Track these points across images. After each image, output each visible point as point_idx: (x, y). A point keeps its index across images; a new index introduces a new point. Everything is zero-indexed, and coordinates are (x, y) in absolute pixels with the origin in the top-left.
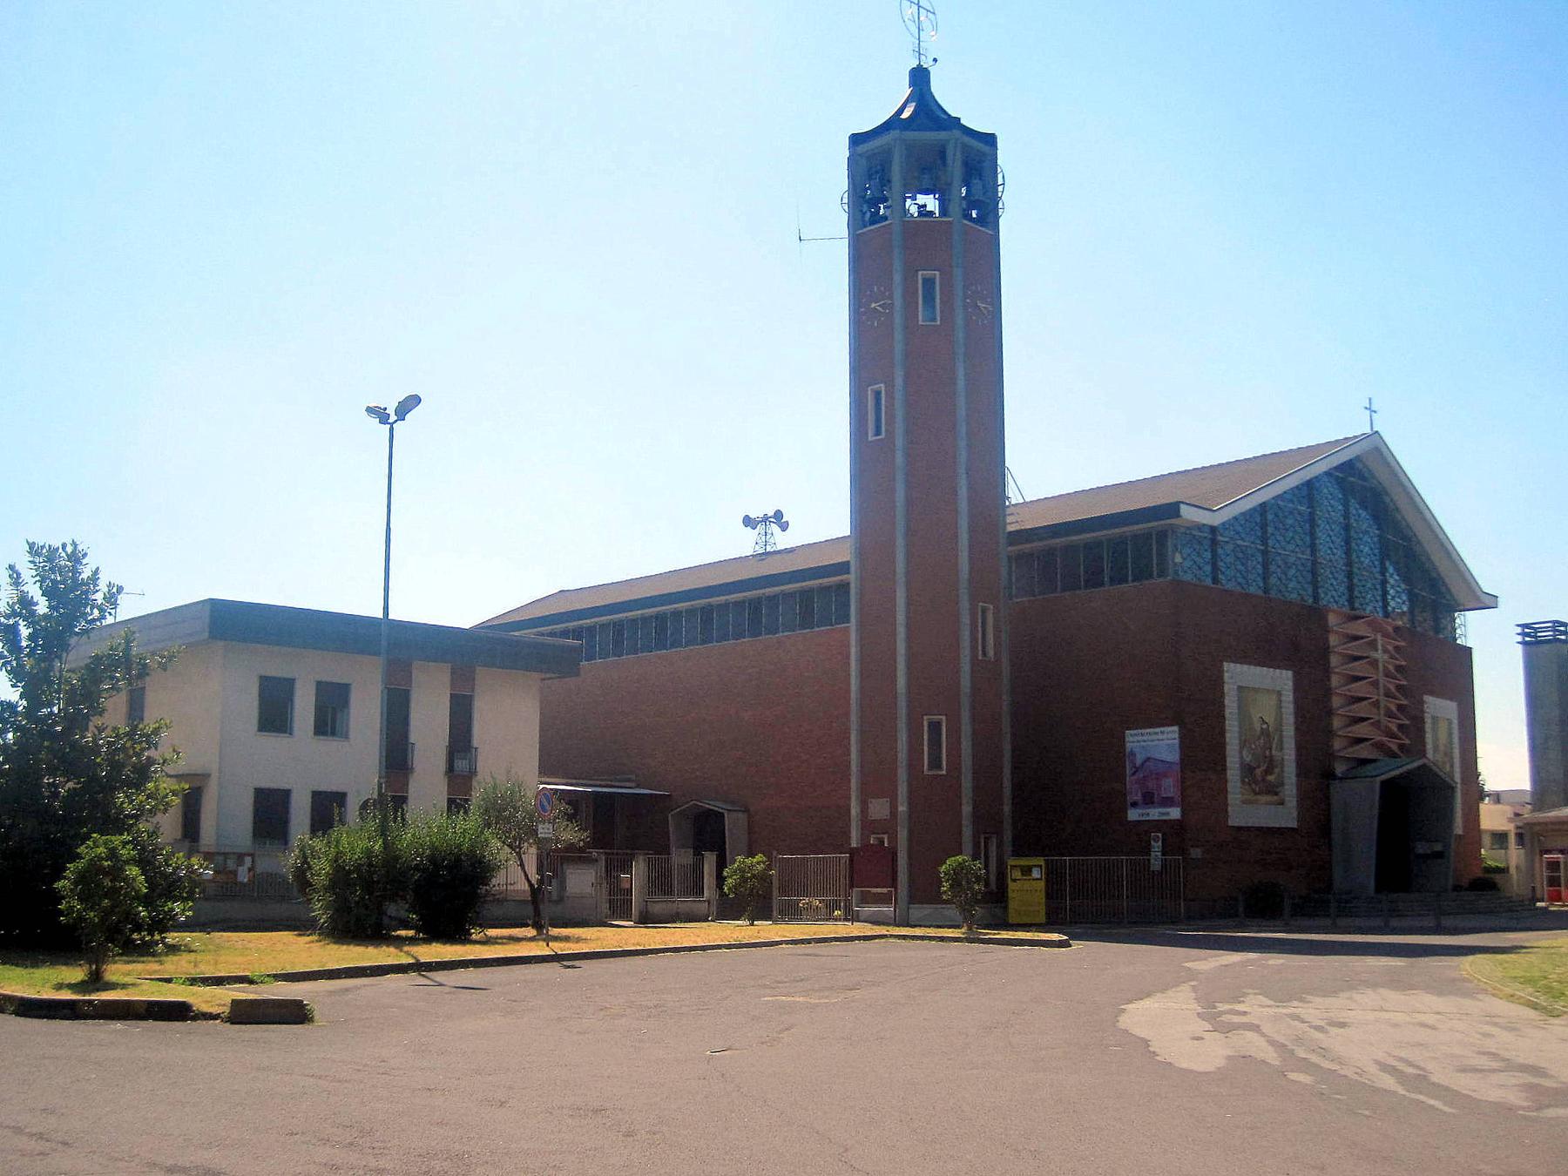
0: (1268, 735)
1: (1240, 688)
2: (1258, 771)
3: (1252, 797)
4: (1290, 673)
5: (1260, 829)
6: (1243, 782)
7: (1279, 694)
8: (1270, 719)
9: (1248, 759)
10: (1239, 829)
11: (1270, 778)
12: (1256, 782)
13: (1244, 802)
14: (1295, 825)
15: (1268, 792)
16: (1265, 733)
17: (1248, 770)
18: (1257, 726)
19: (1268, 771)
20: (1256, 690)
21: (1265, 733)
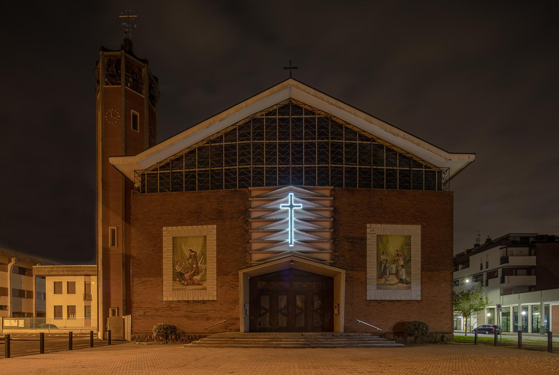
0: (195, 257)
1: (173, 238)
2: (187, 276)
3: (180, 287)
4: (215, 226)
5: (188, 302)
6: (174, 280)
7: (205, 237)
8: (198, 250)
9: (178, 269)
15: (193, 284)
16: (194, 257)
17: (179, 276)
18: (187, 254)
19: (197, 273)
20: (187, 237)
21: (194, 257)
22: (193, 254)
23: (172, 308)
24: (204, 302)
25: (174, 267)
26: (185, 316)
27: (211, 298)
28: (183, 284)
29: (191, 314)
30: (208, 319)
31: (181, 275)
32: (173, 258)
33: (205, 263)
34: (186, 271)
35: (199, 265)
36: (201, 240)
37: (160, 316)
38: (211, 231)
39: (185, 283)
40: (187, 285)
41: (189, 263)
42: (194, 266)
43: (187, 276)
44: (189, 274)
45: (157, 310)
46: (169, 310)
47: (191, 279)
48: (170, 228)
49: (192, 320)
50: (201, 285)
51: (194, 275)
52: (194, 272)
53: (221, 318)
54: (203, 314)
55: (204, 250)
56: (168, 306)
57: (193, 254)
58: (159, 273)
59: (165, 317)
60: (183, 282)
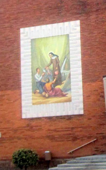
0: (57, 61)
1: (33, 41)
2: (48, 86)
3: (41, 100)
4: (78, 22)
5: (50, 118)
6: (35, 92)
7: (68, 36)
8: (59, 52)
9: (38, 78)
10: (32, 119)
11: (58, 87)
12: (45, 91)
13: (33, 104)
14: (82, 112)
15: (56, 96)
18: (48, 59)
19: (59, 81)
22: (54, 58)
23: (32, 127)
24: (69, 118)
25: (33, 75)
26: (48, 137)
27: (76, 113)
28: (44, 96)
29: (54, 133)
30: (75, 139)
31: (42, 84)
32: (32, 65)
33: (69, 69)
34: (47, 80)
35: (62, 71)
36: (63, 40)
37: (19, 139)
38: (73, 28)
39: (47, 95)
40: (49, 96)
41: (50, 70)
42: (56, 73)
43: (48, 86)
44: (50, 83)
45: (15, 131)
46: (29, 130)
47: (52, 89)
48: (27, 29)
49: (57, 141)
50: (64, 96)
51: (57, 83)
52: (56, 81)
53: (89, 138)
54: (68, 132)
55: (67, 53)
56: (28, 125)
57: (54, 58)
58: (17, 86)
59: (26, 139)
60: (44, 93)
